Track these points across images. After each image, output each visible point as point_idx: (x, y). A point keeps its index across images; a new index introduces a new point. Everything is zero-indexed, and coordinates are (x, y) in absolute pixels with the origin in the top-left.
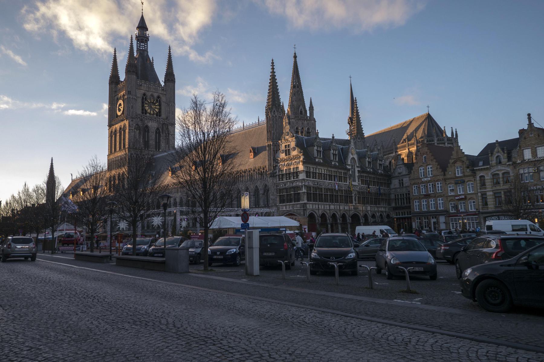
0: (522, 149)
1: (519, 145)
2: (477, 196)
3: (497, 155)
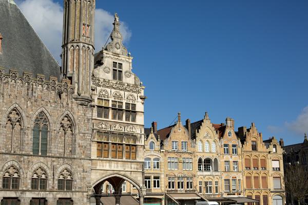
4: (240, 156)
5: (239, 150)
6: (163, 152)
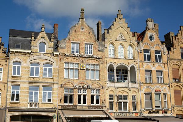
0: (71, 41)
1: (68, 37)
2: (6, 86)
3: (41, 40)
4: (166, 65)
5: (164, 58)
6: (57, 55)
